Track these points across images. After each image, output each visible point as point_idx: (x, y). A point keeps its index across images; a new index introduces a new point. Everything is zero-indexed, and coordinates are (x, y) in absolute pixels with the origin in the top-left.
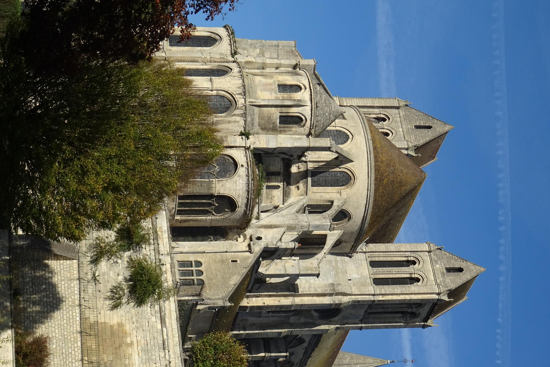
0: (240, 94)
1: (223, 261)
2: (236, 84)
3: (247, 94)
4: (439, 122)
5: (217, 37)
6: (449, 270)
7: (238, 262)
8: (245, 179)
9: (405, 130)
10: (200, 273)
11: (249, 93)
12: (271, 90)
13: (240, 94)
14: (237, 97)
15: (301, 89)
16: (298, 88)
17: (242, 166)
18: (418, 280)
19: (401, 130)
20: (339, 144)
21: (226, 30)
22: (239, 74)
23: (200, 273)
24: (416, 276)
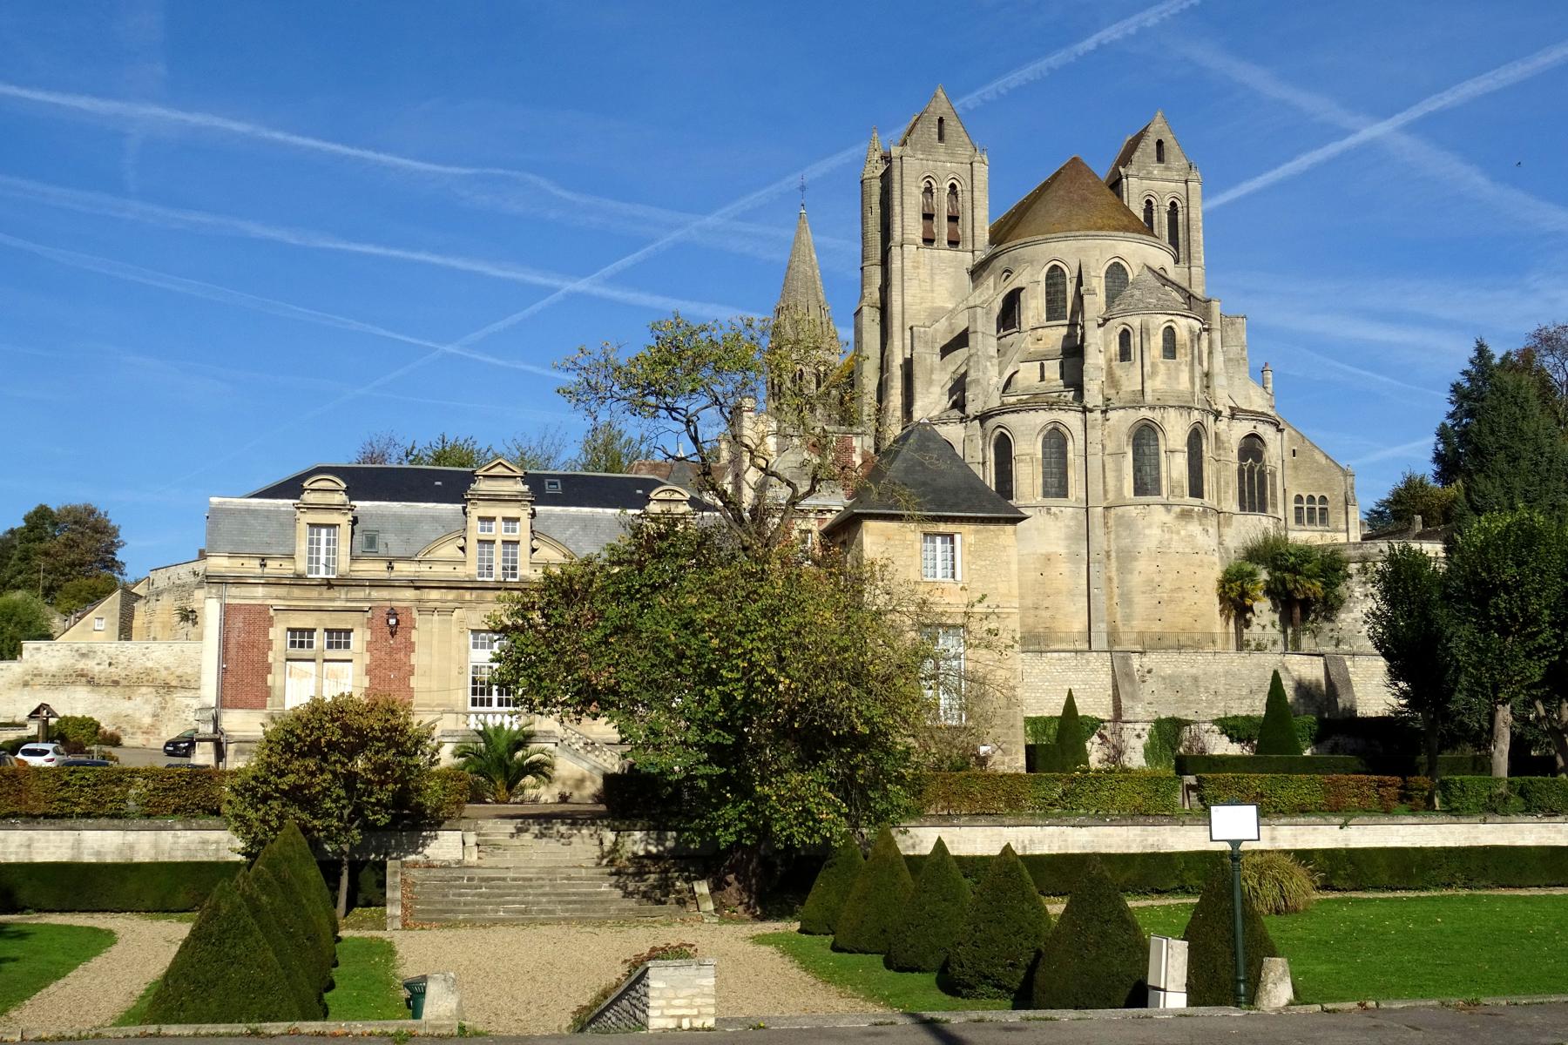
0: (1189, 413)
1: (1296, 468)
2: (1176, 417)
3: (1190, 405)
4: (933, 104)
5: (1050, 427)
6: (1160, 159)
7: (1295, 448)
8: (1267, 426)
9: (948, 158)
10: (1311, 499)
11: (1186, 402)
12: (1177, 370)
13: (1189, 413)
14: (1193, 420)
15: (1170, 327)
16: (1170, 334)
17: (1255, 427)
18: (1173, 204)
19: (949, 165)
20: (1127, 279)
21: (1031, 412)
22: (1157, 411)
23: (1311, 499)
24: (1168, 204)
